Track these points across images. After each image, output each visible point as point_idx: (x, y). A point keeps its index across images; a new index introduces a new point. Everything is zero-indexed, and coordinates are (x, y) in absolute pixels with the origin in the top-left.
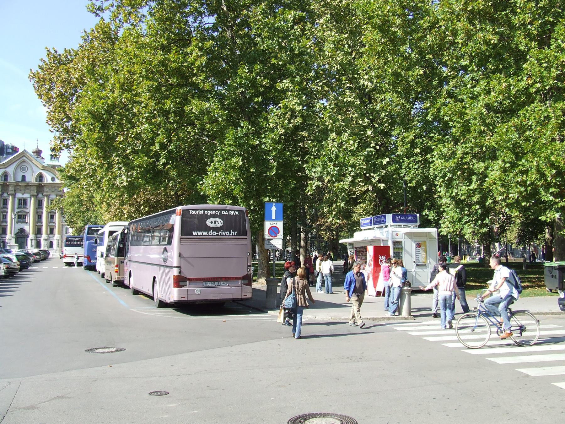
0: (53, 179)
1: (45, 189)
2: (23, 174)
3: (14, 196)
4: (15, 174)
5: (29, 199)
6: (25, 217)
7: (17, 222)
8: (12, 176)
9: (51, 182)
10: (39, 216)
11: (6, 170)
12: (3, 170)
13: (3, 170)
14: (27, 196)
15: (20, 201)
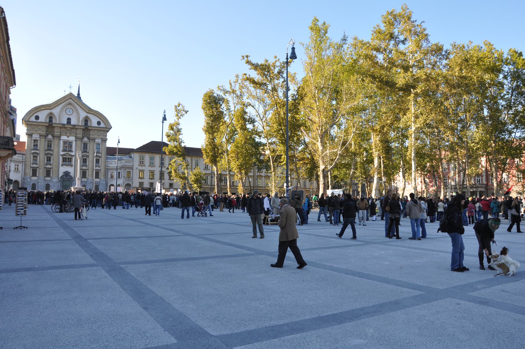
0: (99, 123)
1: (92, 133)
2: (68, 117)
3: (59, 137)
4: (59, 116)
5: (74, 142)
6: (70, 160)
7: (62, 165)
8: (58, 117)
9: (97, 126)
10: (84, 159)
11: (52, 111)
12: (49, 111)
13: (49, 111)
14: (72, 139)
15: (65, 142)
